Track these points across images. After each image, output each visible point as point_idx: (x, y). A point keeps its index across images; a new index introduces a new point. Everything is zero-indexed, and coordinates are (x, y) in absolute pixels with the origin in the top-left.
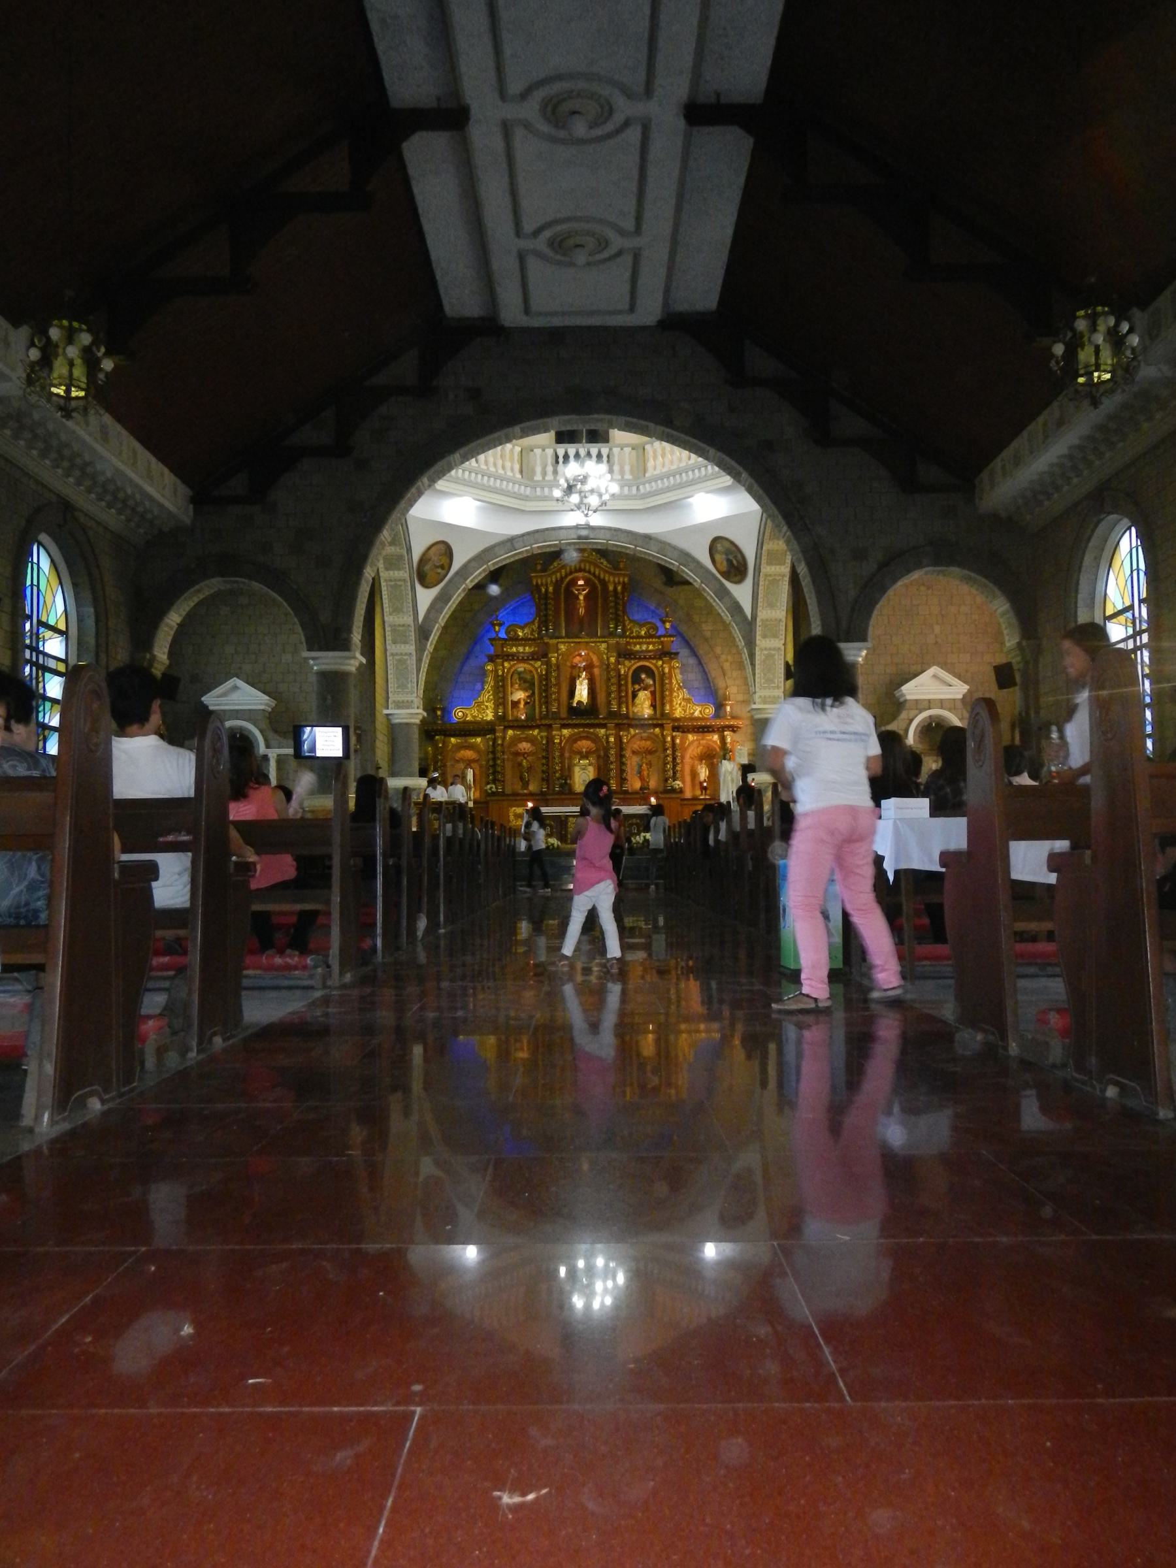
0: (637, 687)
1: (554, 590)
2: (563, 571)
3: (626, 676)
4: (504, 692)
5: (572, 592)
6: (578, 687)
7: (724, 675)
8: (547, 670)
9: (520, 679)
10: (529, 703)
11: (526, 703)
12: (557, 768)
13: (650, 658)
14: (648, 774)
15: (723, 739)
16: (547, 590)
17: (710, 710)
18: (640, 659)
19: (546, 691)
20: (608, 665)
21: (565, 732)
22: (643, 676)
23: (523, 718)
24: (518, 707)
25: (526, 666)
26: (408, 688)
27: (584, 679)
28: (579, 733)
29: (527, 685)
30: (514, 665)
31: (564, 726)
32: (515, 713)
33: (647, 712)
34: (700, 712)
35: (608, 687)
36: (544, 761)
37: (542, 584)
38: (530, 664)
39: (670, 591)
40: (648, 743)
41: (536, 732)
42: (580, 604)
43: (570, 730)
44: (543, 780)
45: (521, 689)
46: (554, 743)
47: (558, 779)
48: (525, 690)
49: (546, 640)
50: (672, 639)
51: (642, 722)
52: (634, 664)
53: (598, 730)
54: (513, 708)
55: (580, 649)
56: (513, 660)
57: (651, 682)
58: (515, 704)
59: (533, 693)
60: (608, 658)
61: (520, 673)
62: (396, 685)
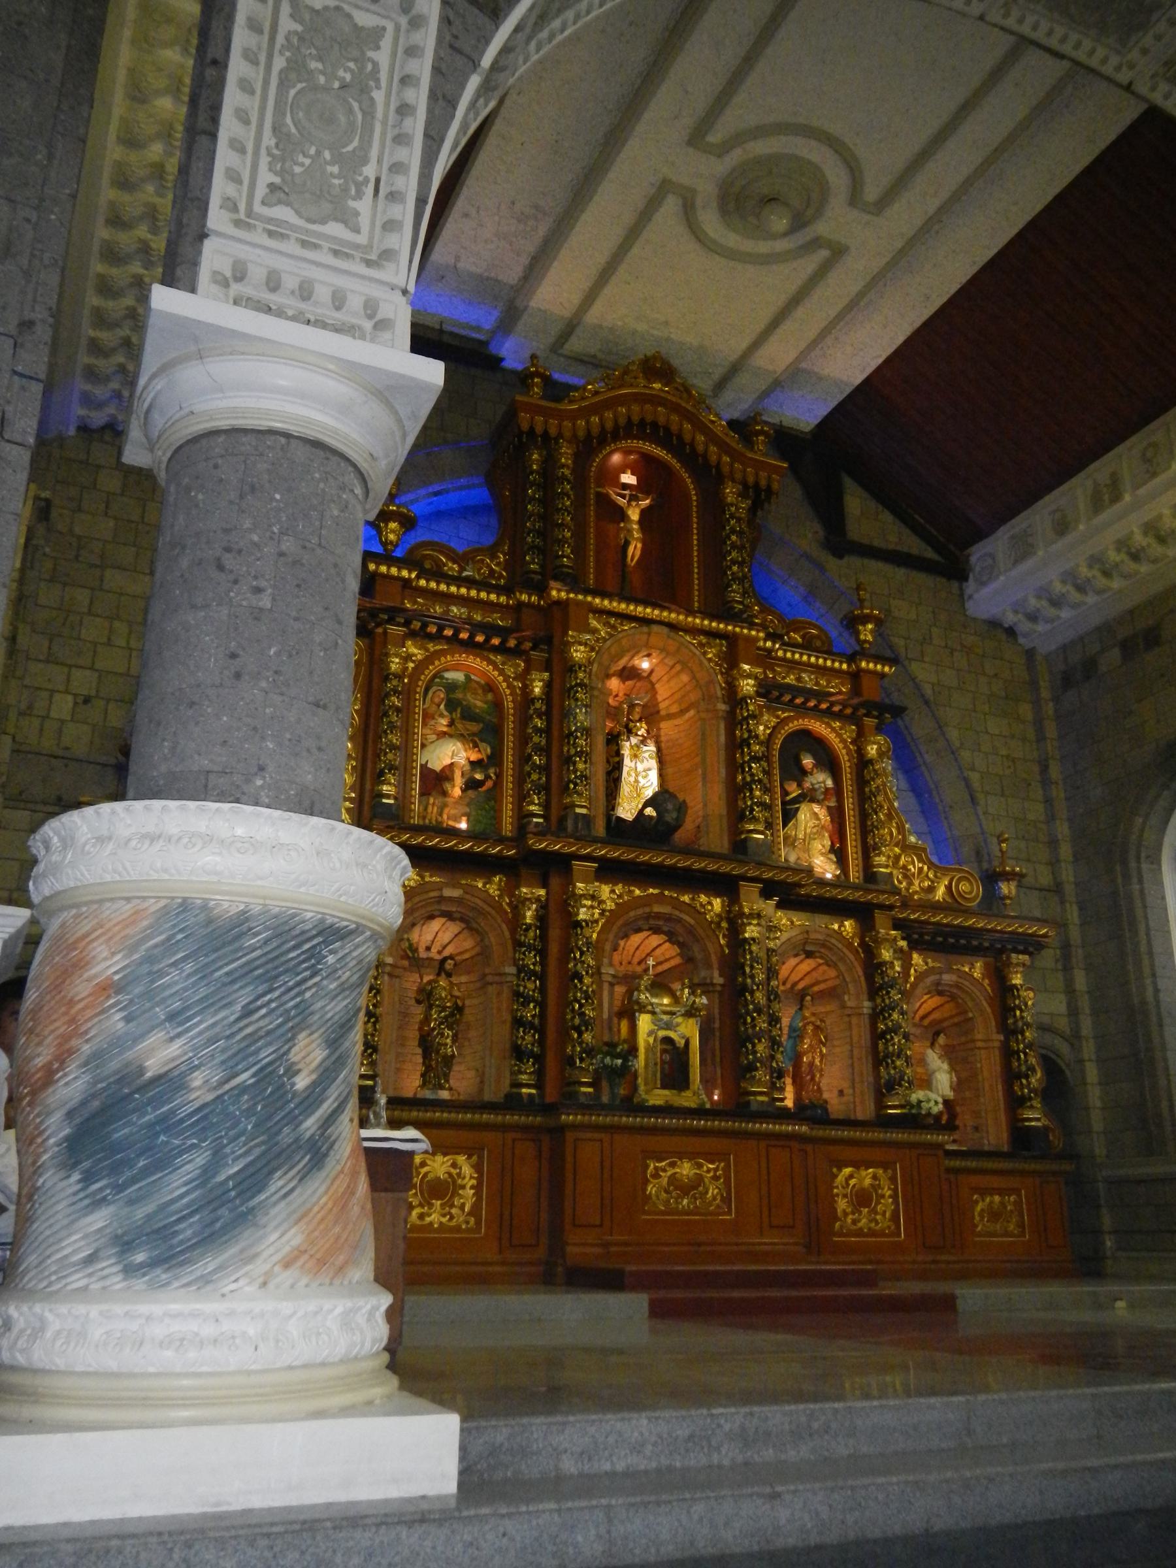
0: (794, 790)
1: (577, 456)
2: (609, 415)
3: (767, 757)
4: (407, 732)
5: (607, 496)
6: (628, 762)
7: (973, 800)
8: (548, 686)
9: (451, 705)
10: (481, 784)
11: (471, 785)
12: (589, 1013)
13: (829, 714)
14: (821, 1061)
15: (999, 976)
16: (550, 462)
17: (972, 890)
18: (803, 711)
19: (546, 751)
20: (734, 699)
21: (605, 890)
22: (808, 761)
23: (463, 826)
24: (445, 794)
25: (474, 662)
26: (349, 219)
27: (643, 742)
28: (647, 901)
29: (474, 727)
30: (443, 653)
31: (608, 871)
32: (433, 811)
33: (825, 868)
34: (949, 888)
35: (734, 767)
36: (531, 986)
37: (546, 434)
38: (490, 662)
39: (832, 563)
40: (808, 965)
41: (494, 887)
42: (630, 531)
43: (619, 889)
44: (518, 1053)
45: (461, 737)
46: (578, 924)
47: (590, 1052)
48: (471, 740)
49: (557, 593)
50: (887, 669)
51: (829, 893)
52: (783, 722)
53: (703, 898)
54: (424, 793)
55: (647, 645)
56: (438, 637)
57: (830, 783)
58: (436, 781)
59: (495, 759)
60: (731, 688)
61: (451, 687)
62: (266, 177)
